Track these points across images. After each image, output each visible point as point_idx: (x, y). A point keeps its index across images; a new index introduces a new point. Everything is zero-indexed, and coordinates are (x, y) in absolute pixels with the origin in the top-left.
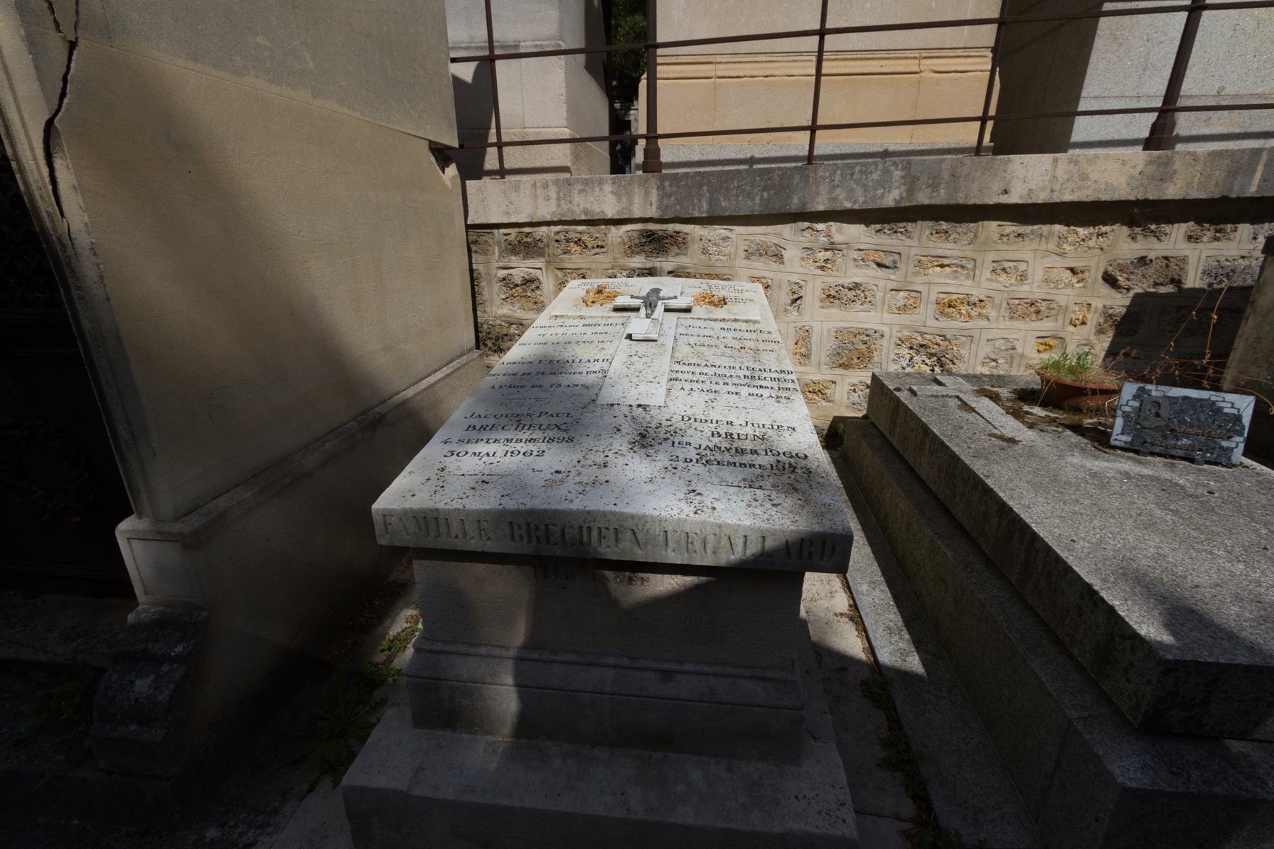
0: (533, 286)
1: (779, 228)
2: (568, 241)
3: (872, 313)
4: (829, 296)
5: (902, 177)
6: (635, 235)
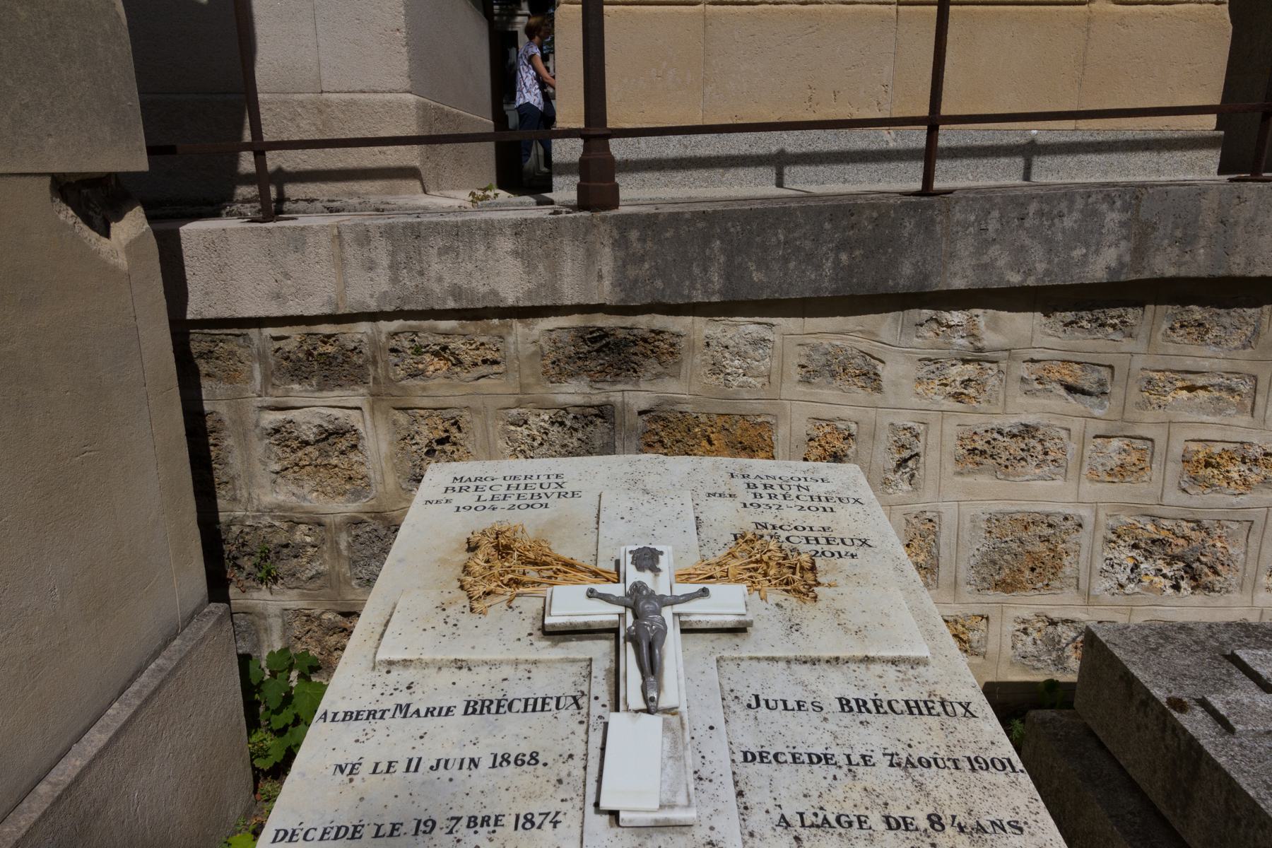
0: (344, 444)
1: (869, 320)
2: (418, 351)
3: (1059, 482)
4: (972, 451)
5: (1123, 224)
6: (567, 337)
